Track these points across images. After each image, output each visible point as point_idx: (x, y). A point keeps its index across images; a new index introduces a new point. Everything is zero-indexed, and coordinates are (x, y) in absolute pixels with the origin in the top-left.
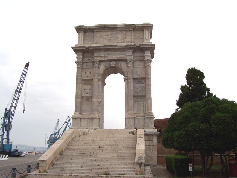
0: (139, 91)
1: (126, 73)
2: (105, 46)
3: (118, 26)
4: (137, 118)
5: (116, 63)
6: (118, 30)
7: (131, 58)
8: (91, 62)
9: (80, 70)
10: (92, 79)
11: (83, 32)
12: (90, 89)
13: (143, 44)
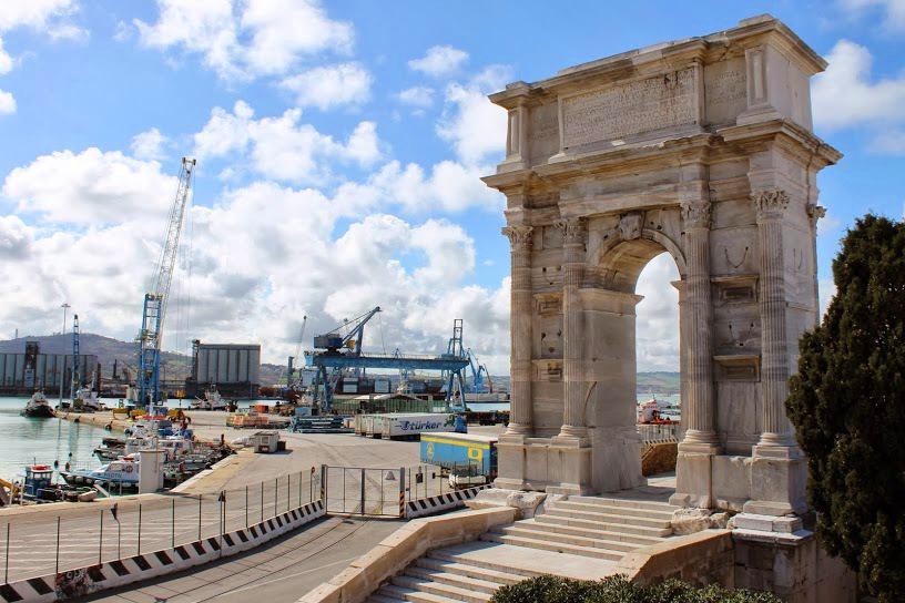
0: (736, 336)
9: (524, 261)
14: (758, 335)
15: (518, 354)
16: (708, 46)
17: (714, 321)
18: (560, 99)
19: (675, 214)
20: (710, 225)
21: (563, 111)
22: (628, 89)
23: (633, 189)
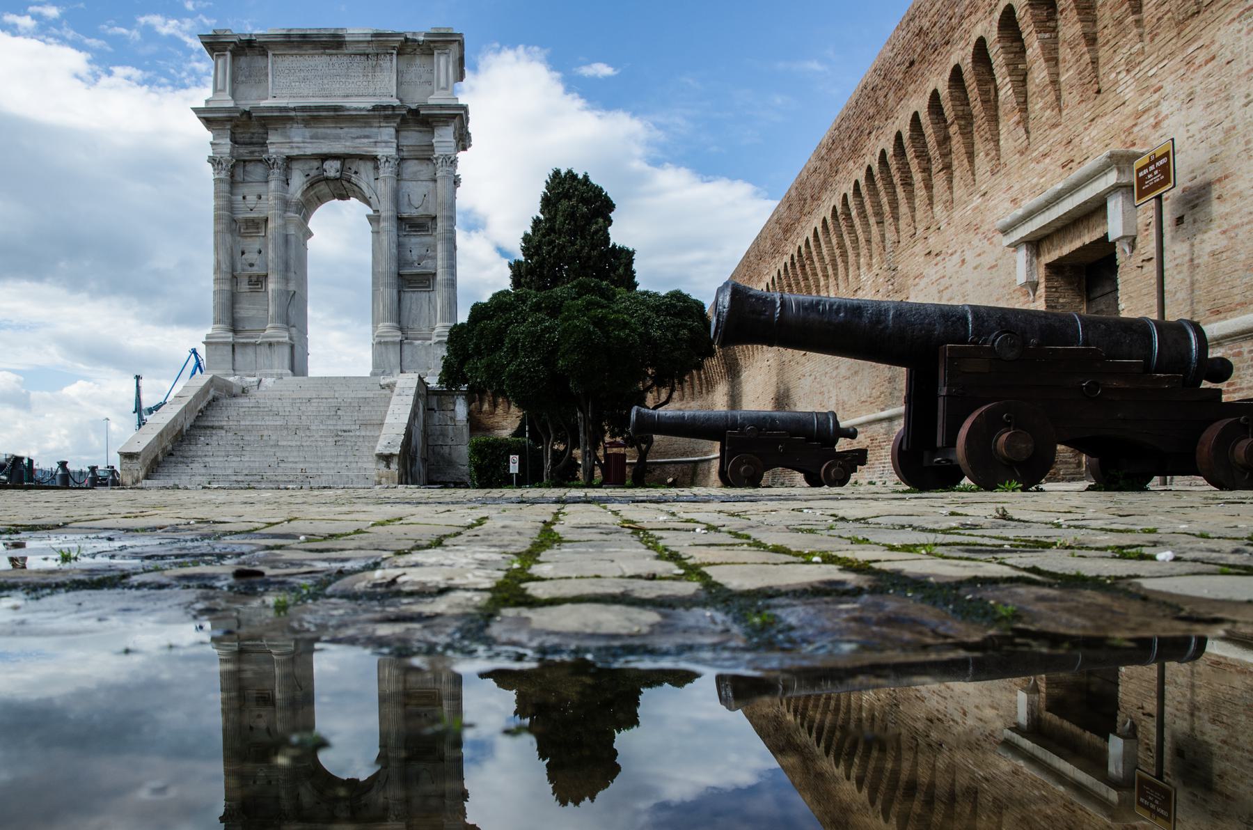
0: (415, 258)
1: (374, 200)
2: (303, 109)
4: (408, 343)
5: (343, 165)
6: (346, 52)
7: (391, 150)
8: (261, 161)
9: (226, 187)
10: (266, 220)
11: (228, 53)
13: (430, 102)
14: (434, 258)
15: (223, 266)
16: (407, 40)
17: (400, 246)
18: (270, 54)
19: (370, 165)
20: (399, 176)
21: (273, 64)
22: (334, 58)
23: (338, 138)
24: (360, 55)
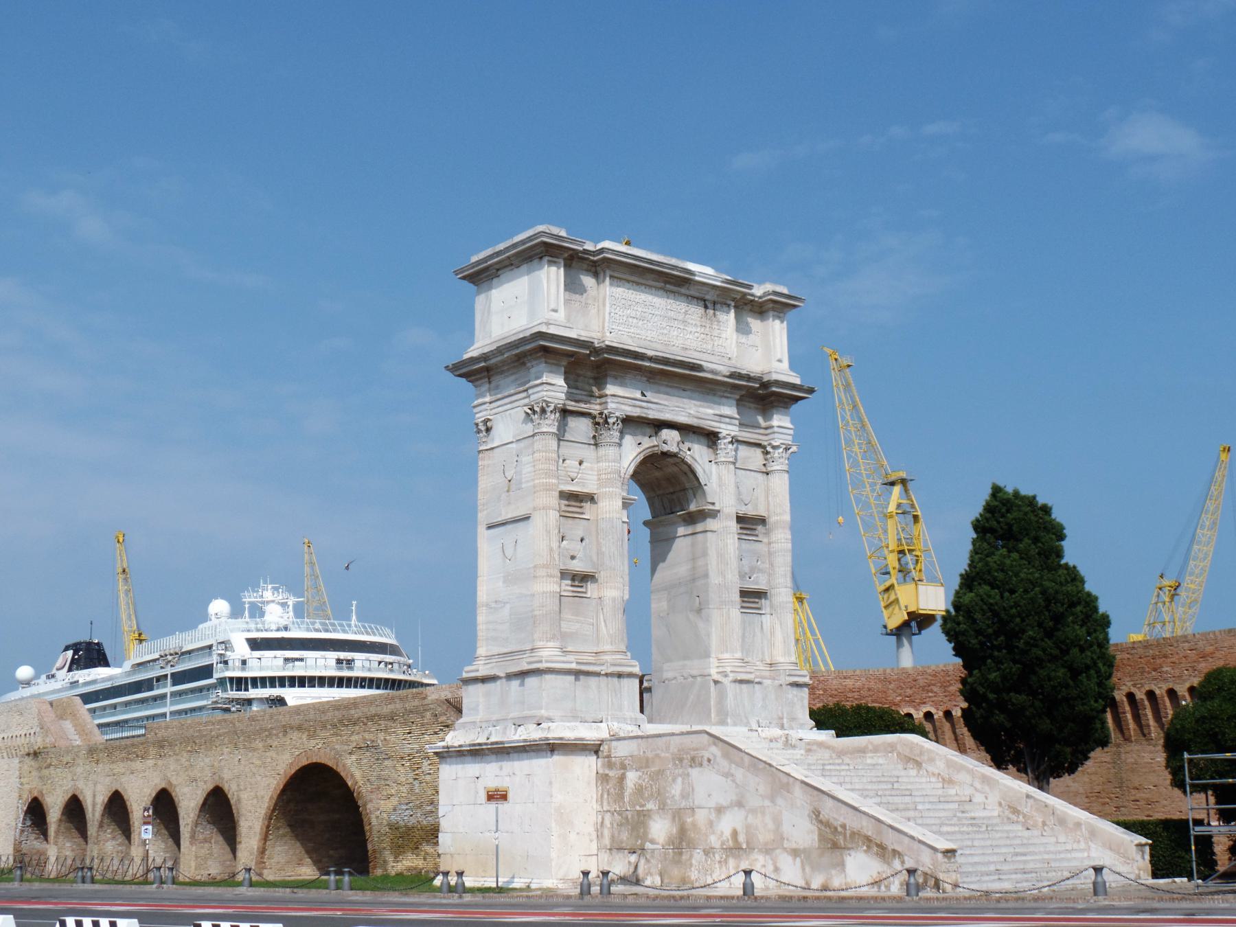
3: (697, 278)
6: (687, 292)
12: (582, 540)
24: (697, 298)
